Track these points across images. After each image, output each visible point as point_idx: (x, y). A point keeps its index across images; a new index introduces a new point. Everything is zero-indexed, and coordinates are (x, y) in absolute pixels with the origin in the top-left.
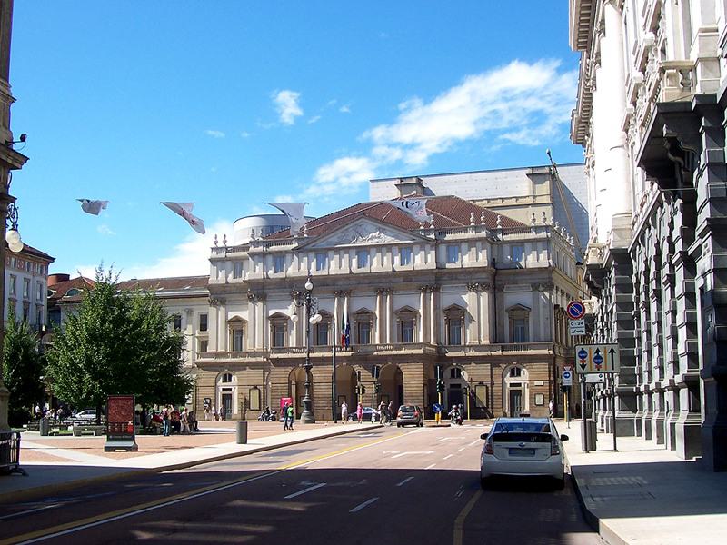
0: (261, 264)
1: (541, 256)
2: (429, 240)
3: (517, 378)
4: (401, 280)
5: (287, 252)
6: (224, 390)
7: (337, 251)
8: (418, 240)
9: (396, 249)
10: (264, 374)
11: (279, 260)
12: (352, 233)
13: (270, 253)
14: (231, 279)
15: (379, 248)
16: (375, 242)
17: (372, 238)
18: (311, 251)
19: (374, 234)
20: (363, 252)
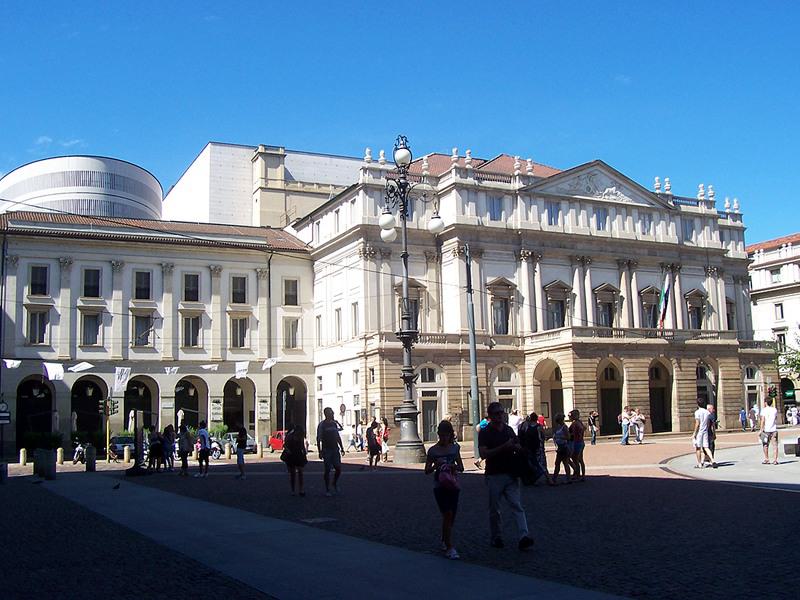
0: (472, 205)
1: (739, 247)
2: (668, 208)
3: (753, 380)
4: (646, 251)
5: (508, 192)
6: (424, 394)
7: (572, 201)
8: (657, 206)
9: (635, 213)
10: (487, 370)
11: (497, 202)
12: (584, 184)
13: (486, 190)
14: (487, 221)
15: (619, 207)
16: (611, 199)
17: (608, 194)
18: (541, 196)
19: (611, 189)
20: (602, 210)
